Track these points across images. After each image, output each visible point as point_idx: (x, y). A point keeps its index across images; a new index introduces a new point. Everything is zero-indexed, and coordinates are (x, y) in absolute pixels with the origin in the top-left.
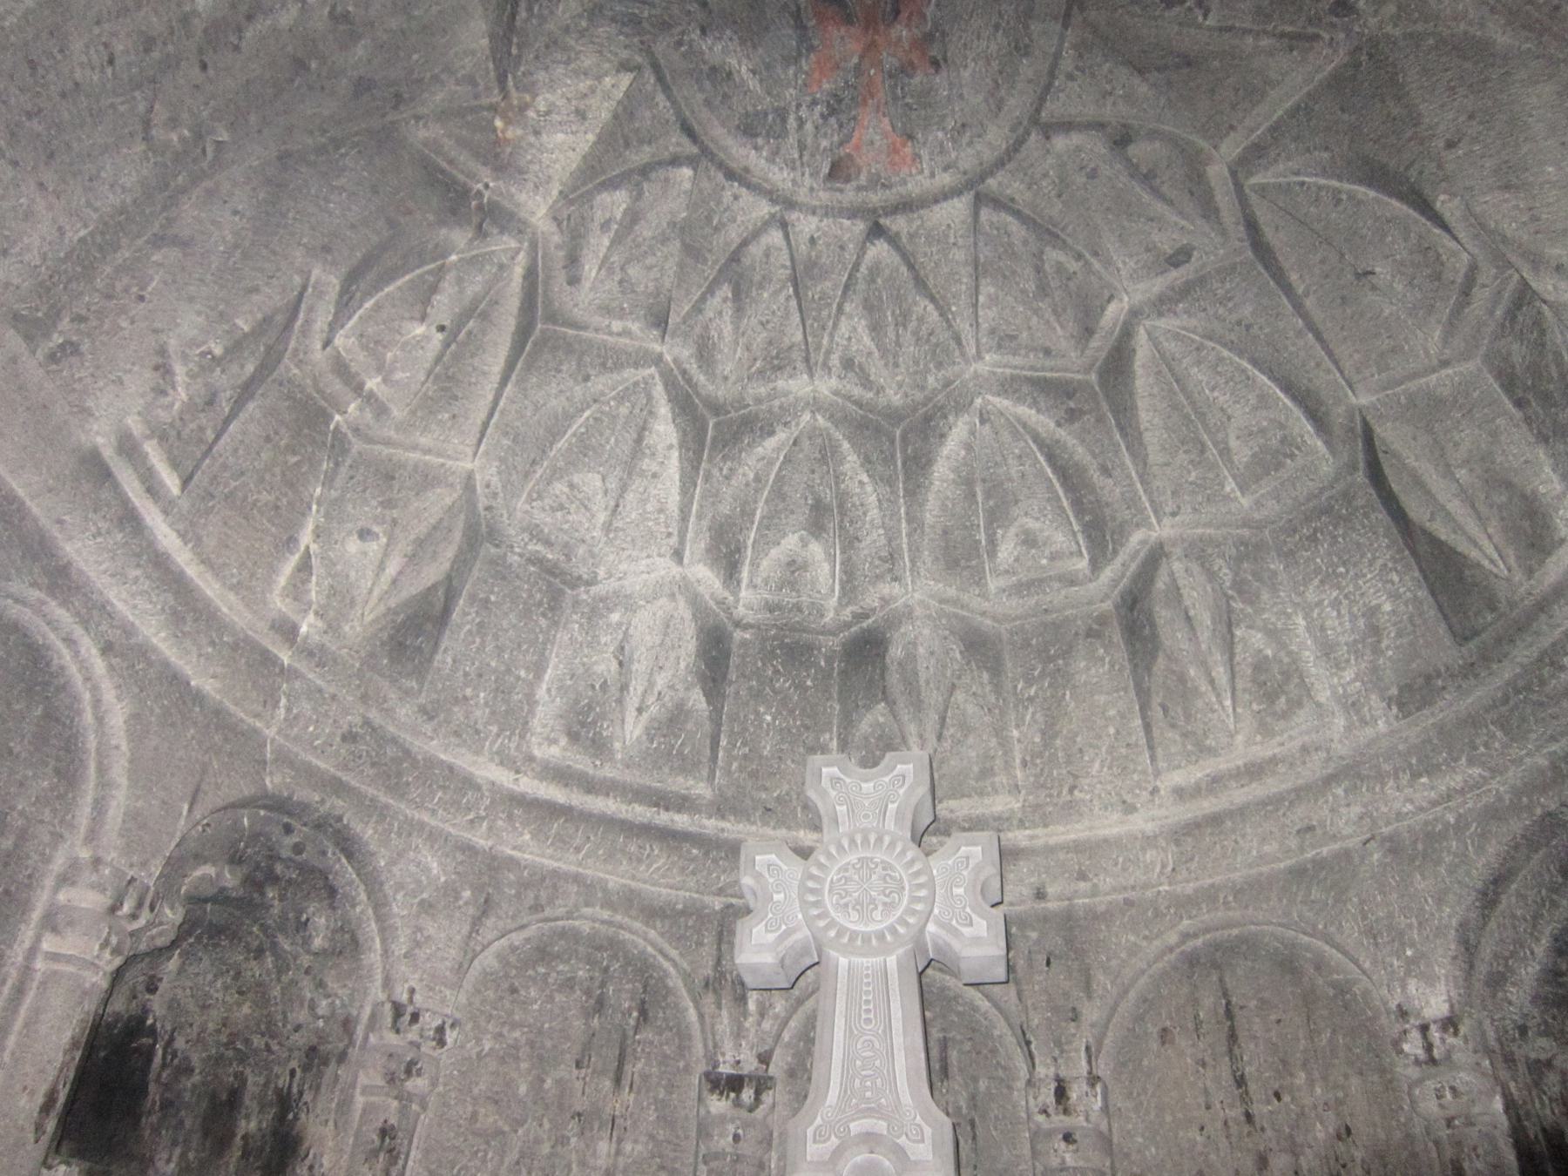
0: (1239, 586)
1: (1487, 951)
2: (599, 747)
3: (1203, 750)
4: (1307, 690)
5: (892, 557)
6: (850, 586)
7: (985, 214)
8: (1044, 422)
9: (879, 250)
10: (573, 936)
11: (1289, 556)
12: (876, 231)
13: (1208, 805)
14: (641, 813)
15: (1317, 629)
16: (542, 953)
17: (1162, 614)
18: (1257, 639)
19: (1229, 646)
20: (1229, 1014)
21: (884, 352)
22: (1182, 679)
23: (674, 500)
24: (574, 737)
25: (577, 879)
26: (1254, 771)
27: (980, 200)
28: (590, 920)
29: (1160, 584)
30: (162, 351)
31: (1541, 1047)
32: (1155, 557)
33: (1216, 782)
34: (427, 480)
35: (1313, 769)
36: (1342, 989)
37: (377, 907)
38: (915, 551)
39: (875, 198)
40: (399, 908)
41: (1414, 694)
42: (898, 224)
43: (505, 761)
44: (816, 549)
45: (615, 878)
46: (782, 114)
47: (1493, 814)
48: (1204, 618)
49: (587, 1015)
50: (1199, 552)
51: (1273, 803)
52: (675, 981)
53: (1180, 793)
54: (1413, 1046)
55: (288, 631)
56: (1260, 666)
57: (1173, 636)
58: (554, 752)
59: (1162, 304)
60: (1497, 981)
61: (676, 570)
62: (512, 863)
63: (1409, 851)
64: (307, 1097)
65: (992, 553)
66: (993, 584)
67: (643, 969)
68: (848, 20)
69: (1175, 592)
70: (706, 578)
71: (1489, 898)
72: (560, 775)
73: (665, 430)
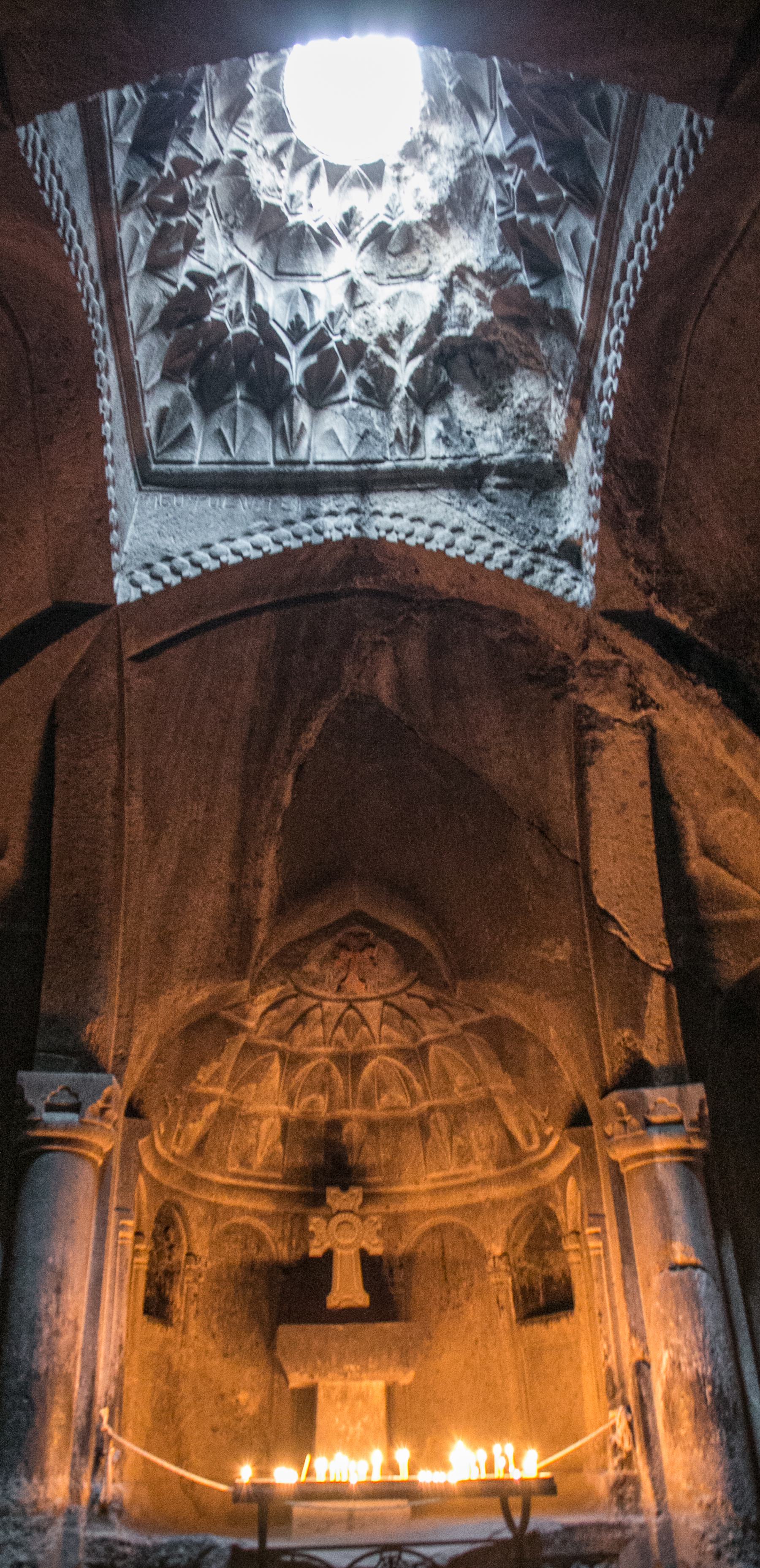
0: (456, 1122)
1: (514, 1235)
2: (249, 1166)
3: (441, 1168)
4: (473, 1157)
5: (346, 1101)
6: (331, 1106)
7: (386, 1008)
8: (400, 1065)
9: (351, 1012)
10: (238, 1225)
11: (470, 1112)
12: (350, 1007)
13: (441, 1184)
14: (260, 1185)
15: (477, 1137)
16: (228, 1232)
17: (433, 1127)
18: (459, 1139)
19: (451, 1139)
20: (443, 1247)
21: (348, 1036)
22: (436, 1147)
23: (277, 1085)
24: (242, 1164)
25: (239, 1207)
26: (456, 1177)
27: (385, 1003)
28: (242, 1220)
29: (432, 1117)
30: (165, 1100)
31: (524, 1264)
32: (431, 1109)
33: (444, 1178)
34: (211, 1098)
35: (473, 1178)
36: (476, 1242)
37: (185, 1225)
38: (354, 1099)
39: (351, 997)
40: (193, 1226)
41: (501, 1164)
42: (359, 1005)
43: (222, 1174)
44: (321, 1098)
45: (251, 1205)
46: (324, 976)
47: (518, 1200)
48: (445, 1131)
49: (242, 1250)
50: (444, 1109)
51: (460, 1187)
52: (268, 1237)
53: (433, 1180)
54: (491, 1263)
55: (174, 1154)
56: (460, 1147)
57: (435, 1134)
58: (235, 1169)
59: (438, 1041)
60: (515, 1245)
61: (275, 1107)
62: (221, 1205)
63: (497, 1205)
64: (168, 1285)
65: (379, 1098)
66: (378, 1107)
67: (257, 1233)
68: (348, 950)
69: (436, 1122)
70: (285, 1109)
71: (515, 1223)
72: (236, 1176)
73: (276, 1065)
